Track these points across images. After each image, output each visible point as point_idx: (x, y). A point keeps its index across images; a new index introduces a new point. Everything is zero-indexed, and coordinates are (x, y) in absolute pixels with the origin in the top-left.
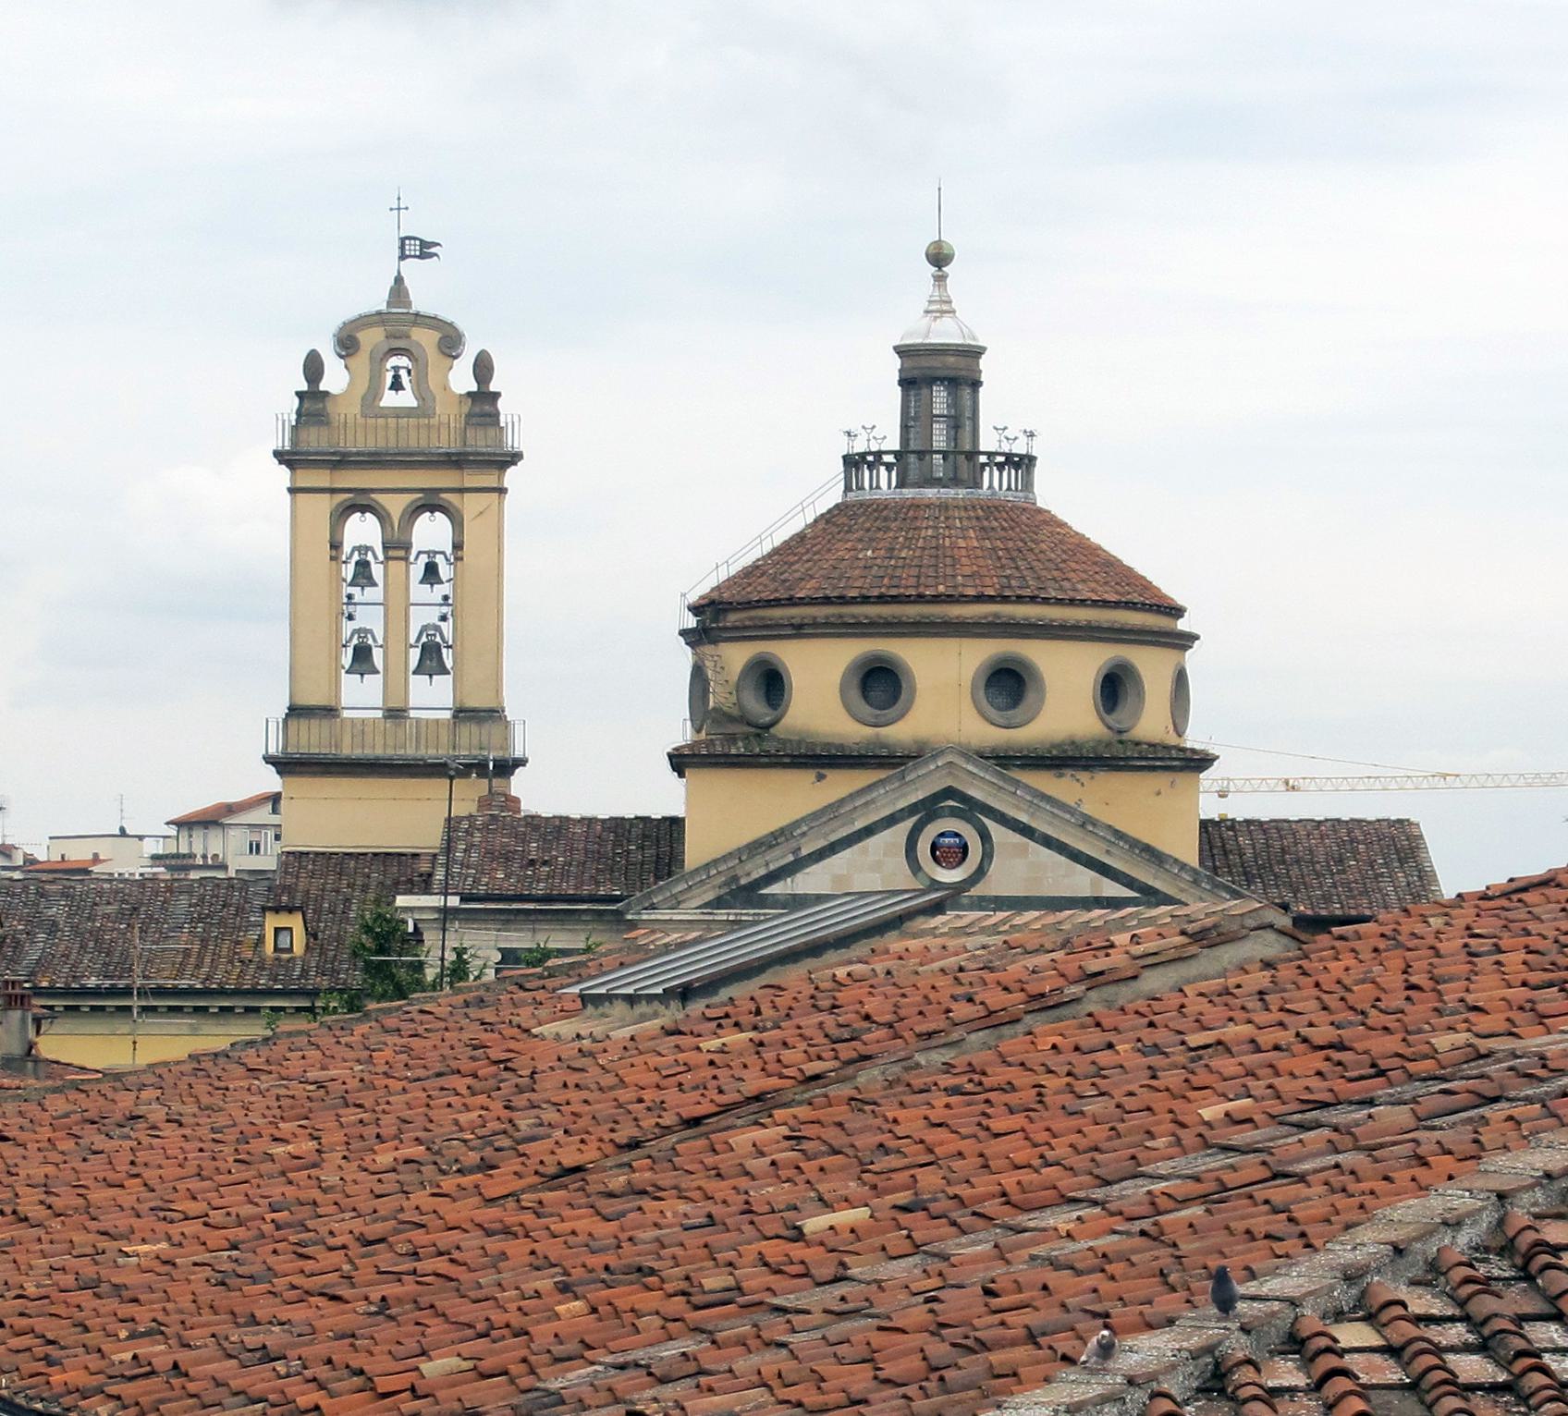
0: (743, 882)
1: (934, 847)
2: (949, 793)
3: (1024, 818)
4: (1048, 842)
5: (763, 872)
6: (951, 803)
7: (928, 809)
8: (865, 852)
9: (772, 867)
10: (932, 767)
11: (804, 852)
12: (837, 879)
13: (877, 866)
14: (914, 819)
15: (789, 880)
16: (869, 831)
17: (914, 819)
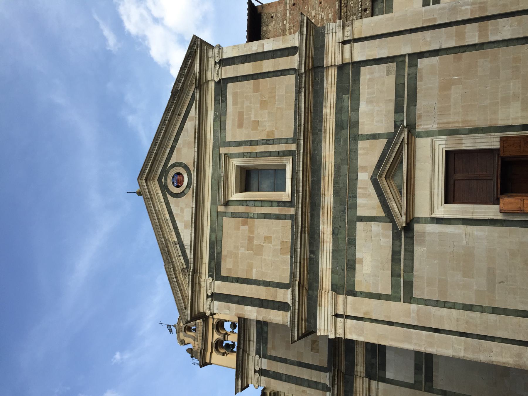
0: (185, 267)
1: (178, 187)
2: (159, 180)
3: (168, 150)
4: (176, 140)
5: (182, 258)
6: (163, 180)
7: (164, 189)
8: (177, 214)
9: (180, 254)
10: (146, 187)
11: (176, 240)
12: (186, 227)
13: (182, 210)
14: (167, 194)
15: (186, 247)
16: (171, 213)
17: (167, 194)
